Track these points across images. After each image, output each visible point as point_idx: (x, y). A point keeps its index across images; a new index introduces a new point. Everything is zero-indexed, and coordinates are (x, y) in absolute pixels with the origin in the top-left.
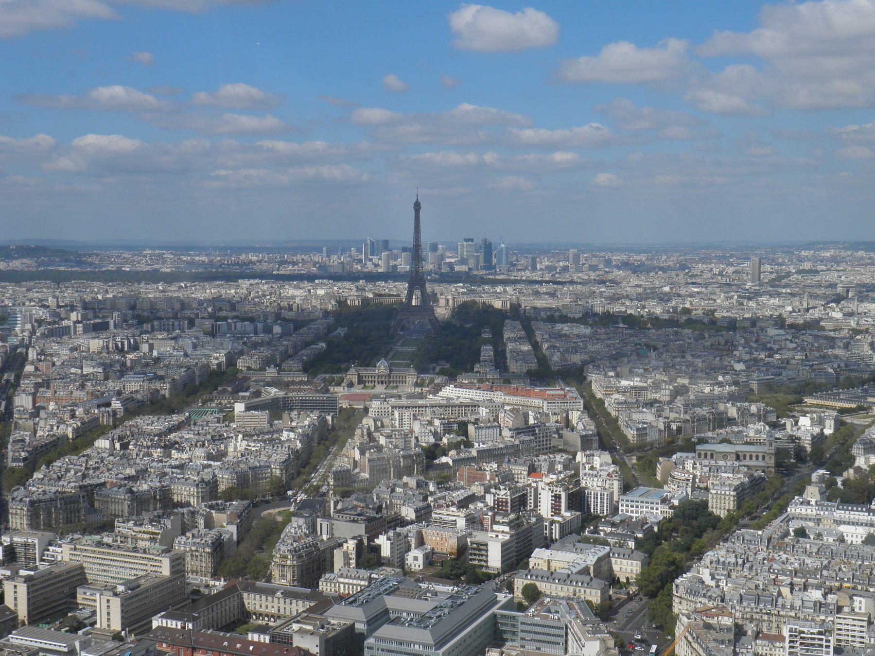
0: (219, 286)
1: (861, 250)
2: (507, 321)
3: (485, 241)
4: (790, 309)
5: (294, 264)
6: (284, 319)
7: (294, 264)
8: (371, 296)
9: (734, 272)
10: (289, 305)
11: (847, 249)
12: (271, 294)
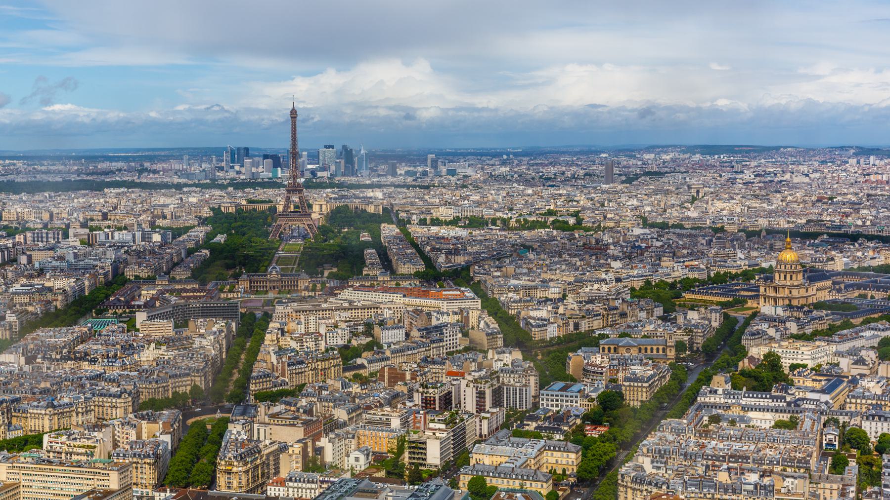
0: (84, 195)
1: (698, 153)
2: (383, 225)
3: (344, 147)
4: (648, 209)
5: (155, 172)
6: (159, 227)
7: (155, 172)
8: (244, 202)
9: (585, 175)
10: (162, 212)
11: (684, 152)
12: (142, 203)
